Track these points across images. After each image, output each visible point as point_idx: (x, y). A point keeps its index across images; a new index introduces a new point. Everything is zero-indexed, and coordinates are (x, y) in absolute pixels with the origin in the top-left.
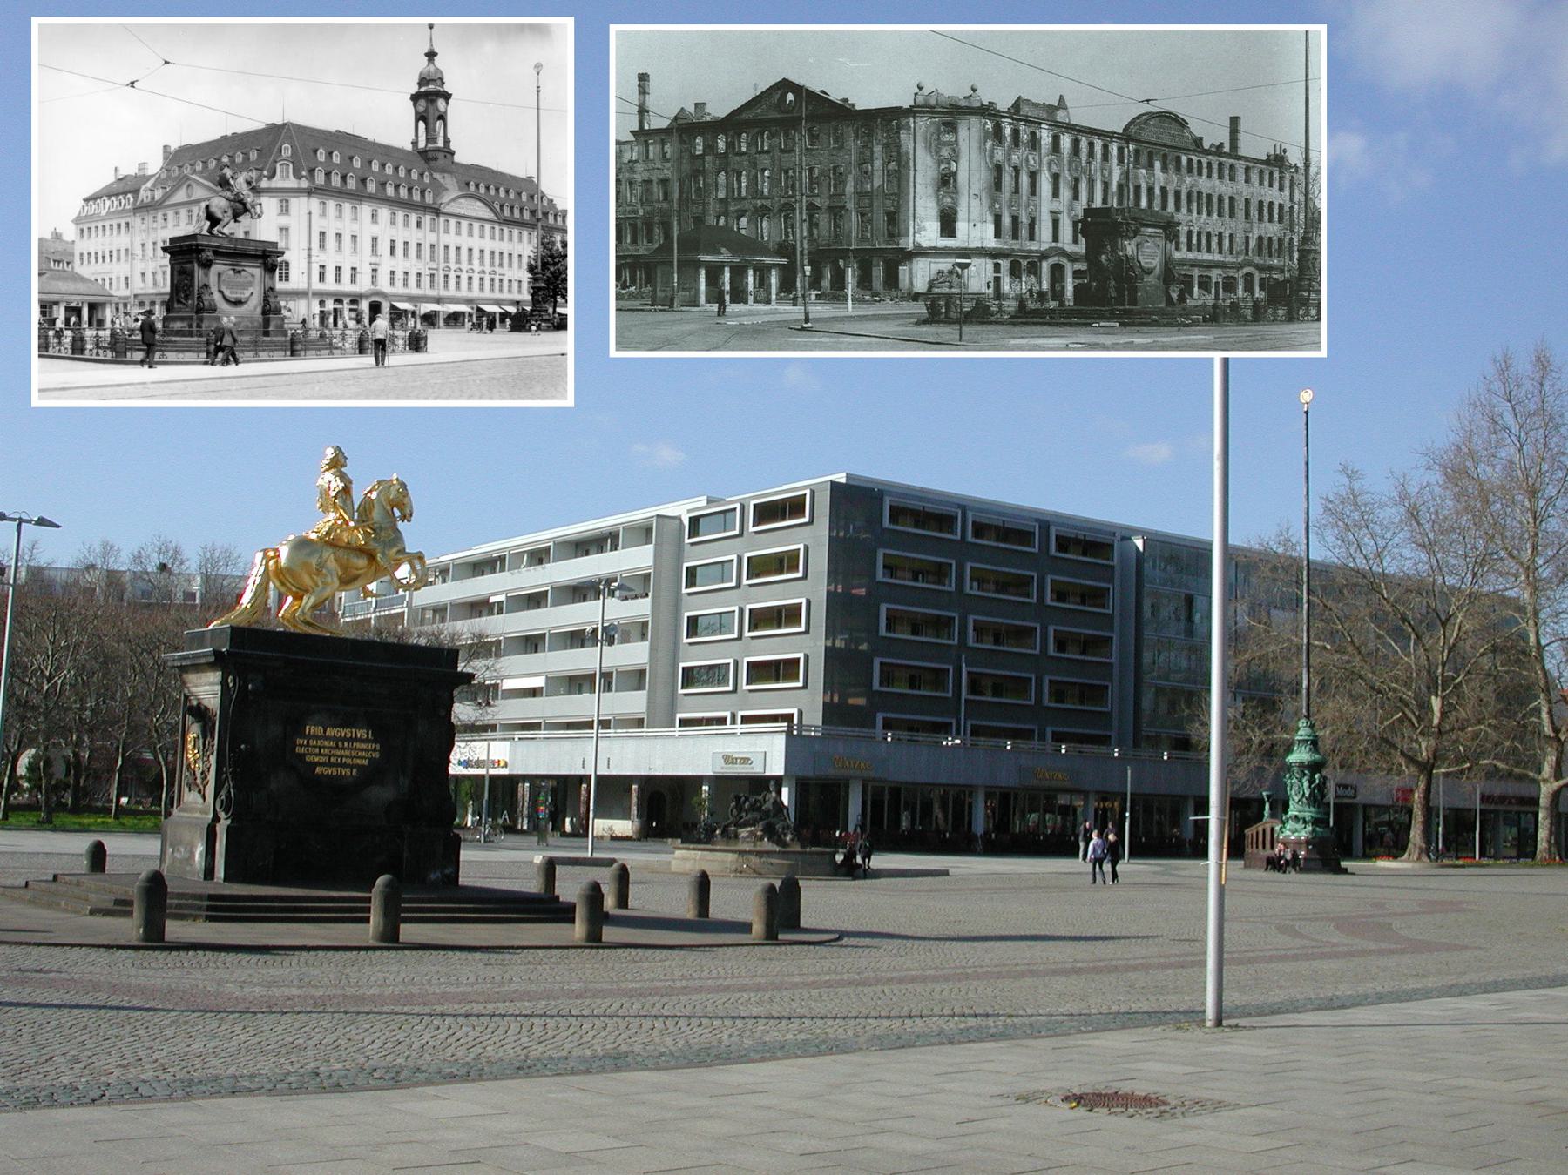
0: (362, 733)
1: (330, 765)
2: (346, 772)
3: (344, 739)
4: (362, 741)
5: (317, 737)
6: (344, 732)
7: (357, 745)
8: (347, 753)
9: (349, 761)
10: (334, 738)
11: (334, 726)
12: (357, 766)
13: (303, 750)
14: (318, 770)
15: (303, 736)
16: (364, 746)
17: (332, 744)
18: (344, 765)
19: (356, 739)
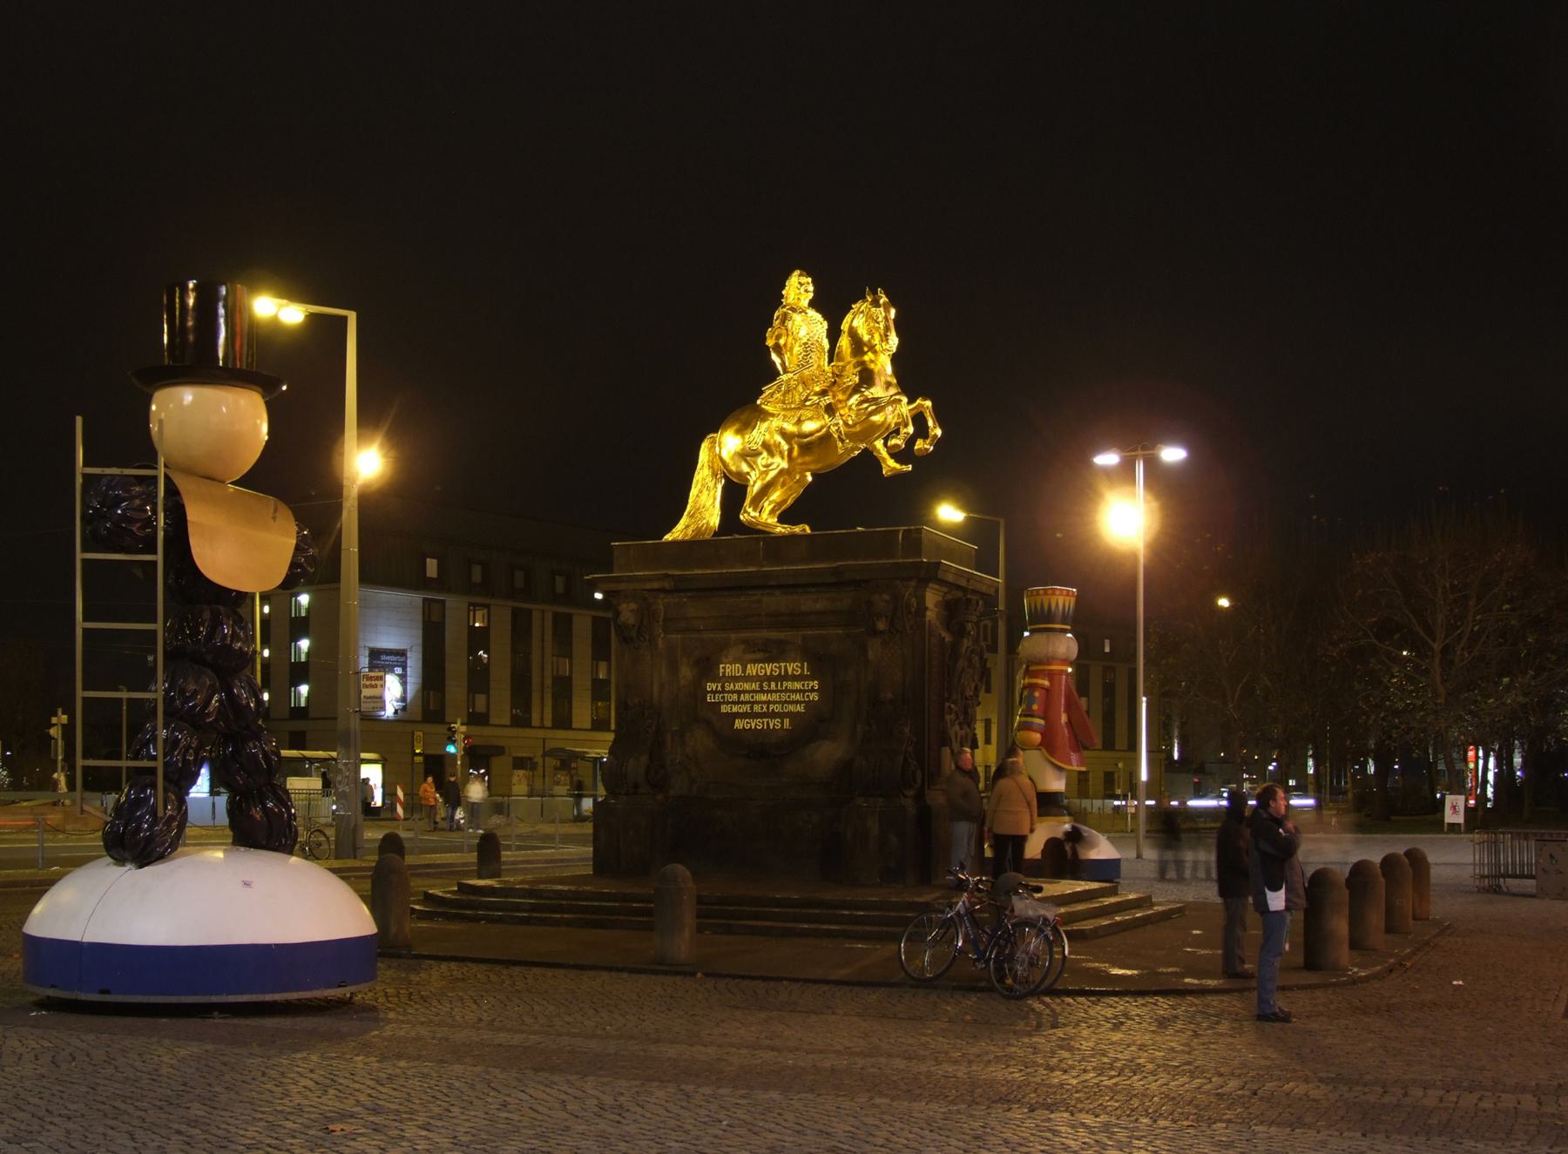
0: (792, 667)
1: (752, 715)
2: (775, 723)
3: (769, 679)
4: (794, 678)
5: (735, 679)
6: (769, 668)
7: (789, 685)
8: (775, 697)
9: (777, 708)
10: (757, 678)
11: (755, 661)
12: (789, 715)
14: (739, 724)
15: (716, 679)
16: (798, 685)
17: (755, 686)
18: (773, 715)
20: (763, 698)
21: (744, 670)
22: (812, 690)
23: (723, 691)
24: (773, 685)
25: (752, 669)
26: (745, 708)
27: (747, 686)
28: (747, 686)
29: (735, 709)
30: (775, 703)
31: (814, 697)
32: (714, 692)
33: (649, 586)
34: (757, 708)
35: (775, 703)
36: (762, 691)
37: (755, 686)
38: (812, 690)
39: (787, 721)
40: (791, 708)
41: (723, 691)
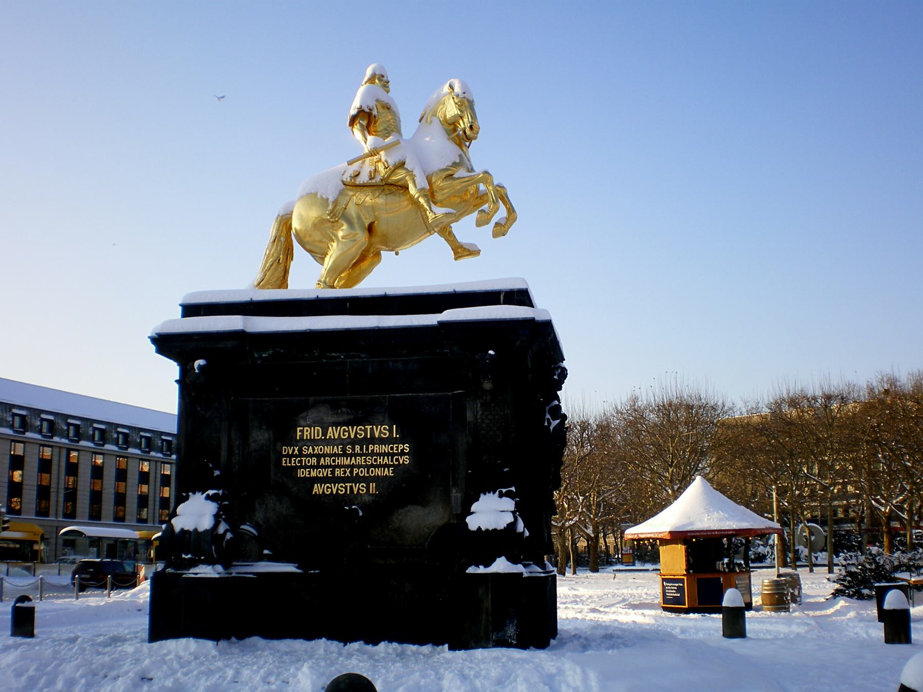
1: (335, 480)
2: (359, 488)
3: (354, 442)
4: (382, 441)
5: (314, 442)
6: (353, 432)
7: (377, 448)
8: (360, 460)
9: (363, 473)
10: (339, 441)
11: (337, 424)
12: (376, 479)
13: (294, 462)
14: (317, 489)
15: (292, 442)
16: (385, 448)
17: (337, 450)
18: (357, 479)
19: (373, 440)
20: (347, 462)
21: (325, 434)
22: (402, 453)
23: (301, 454)
24: (357, 448)
25: (332, 432)
26: (327, 472)
27: (328, 450)
28: (328, 450)
29: (314, 474)
30: (359, 466)
31: (406, 460)
32: (290, 456)
33: (221, 345)
34: (338, 472)
35: (359, 466)
36: (345, 454)
37: (337, 450)
38: (402, 453)
39: (373, 486)
40: (378, 472)
41: (301, 454)
